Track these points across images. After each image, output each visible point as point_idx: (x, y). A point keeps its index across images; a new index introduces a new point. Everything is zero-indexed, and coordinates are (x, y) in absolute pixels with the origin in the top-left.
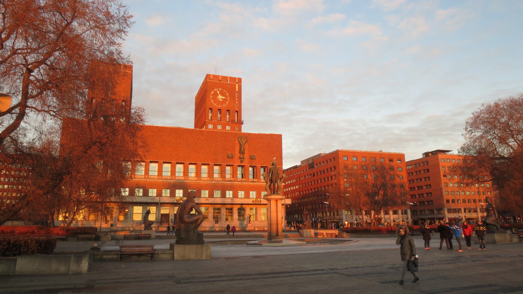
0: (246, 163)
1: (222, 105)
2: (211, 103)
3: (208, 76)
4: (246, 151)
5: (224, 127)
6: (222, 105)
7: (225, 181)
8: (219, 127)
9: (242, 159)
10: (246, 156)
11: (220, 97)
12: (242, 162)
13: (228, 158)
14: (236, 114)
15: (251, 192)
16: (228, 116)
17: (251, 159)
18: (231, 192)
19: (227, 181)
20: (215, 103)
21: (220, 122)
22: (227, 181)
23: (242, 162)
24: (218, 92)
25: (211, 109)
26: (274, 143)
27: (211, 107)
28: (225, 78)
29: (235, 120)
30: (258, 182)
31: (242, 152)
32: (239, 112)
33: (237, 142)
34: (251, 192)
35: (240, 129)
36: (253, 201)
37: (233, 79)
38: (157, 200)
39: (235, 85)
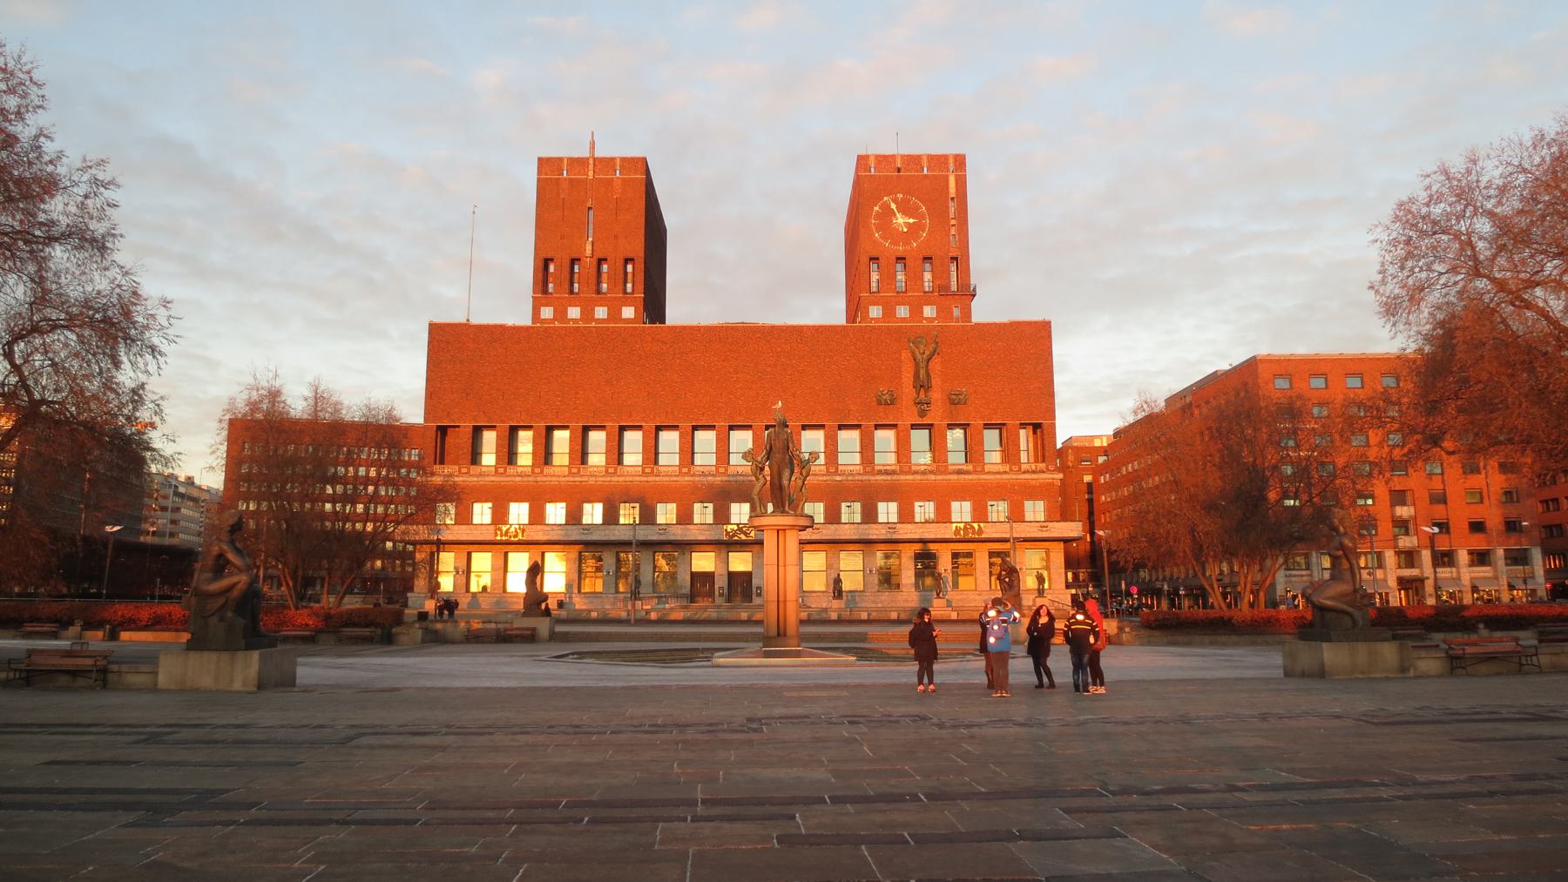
0: (936, 416)
1: (907, 243)
2: (875, 242)
3: (862, 161)
4: (936, 381)
5: (916, 311)
6: (907, 243)
7: (873, 473)
8: (903, 312)
9: (922, 406)
10: (936, 395)
11: (901, 220)
12: (922, 414)
13: (880, 403)
14: (953, 267)
15: (955, 505)
16: (928, 276)
17: (952, 403)
18: (893, 506)
19: (880, 472)
20: (885, 238)
21: (901, 298)
22: (880, 472)
23: (922, 414)
24: (893, 206)
25: (874, 259)
26: (1029, 345)
27: (875, 254)
28: (914, 161)
29: (948, 287)
30: (975, 472)
31: (922, 385)
32: (960, 259)
33: (905, 355)
34: (955, 505)
35: (967, 313)
36: (957, 530)
37: (939, 161)
38: (678, 533)
39: (946, 179)
